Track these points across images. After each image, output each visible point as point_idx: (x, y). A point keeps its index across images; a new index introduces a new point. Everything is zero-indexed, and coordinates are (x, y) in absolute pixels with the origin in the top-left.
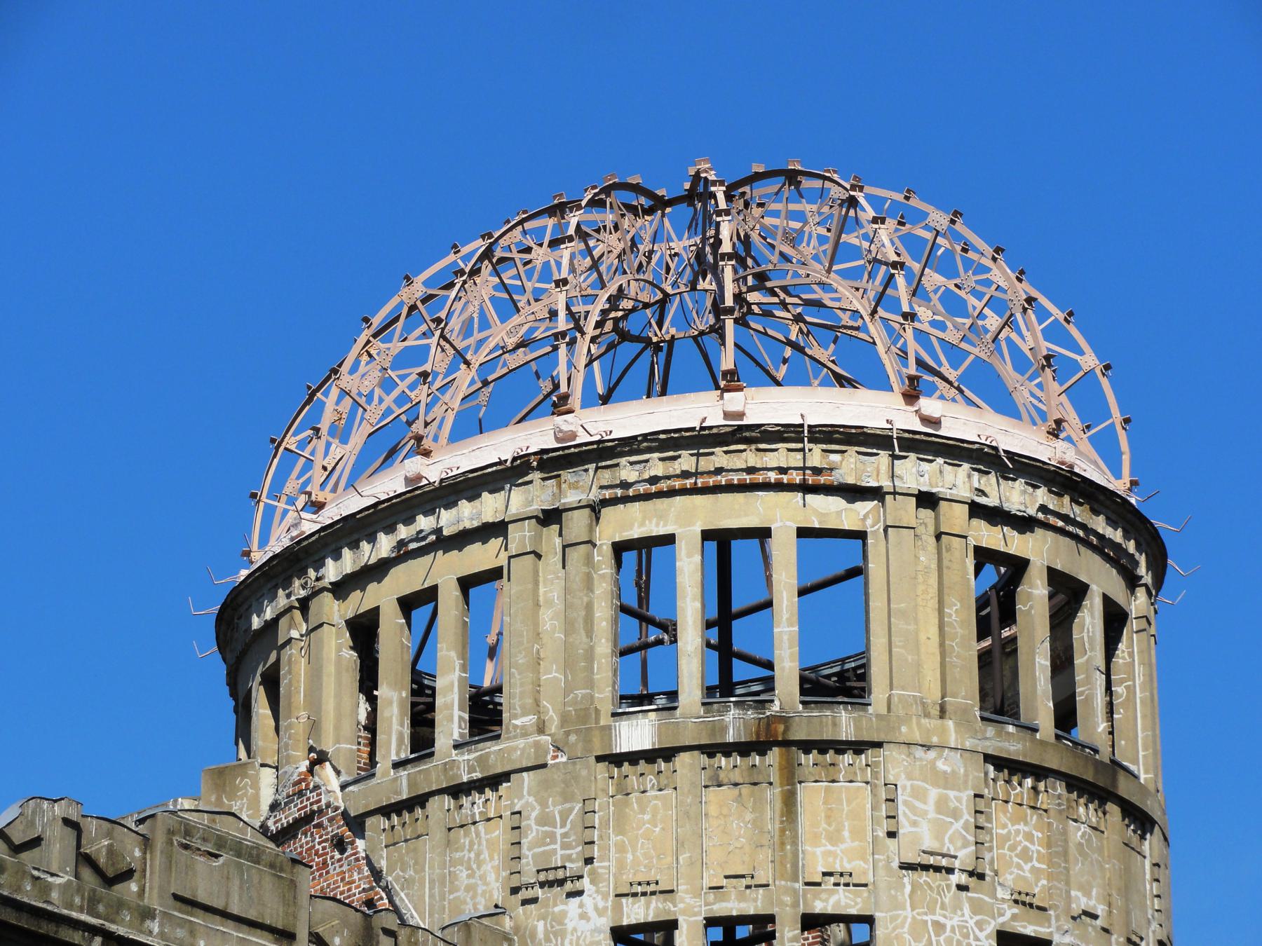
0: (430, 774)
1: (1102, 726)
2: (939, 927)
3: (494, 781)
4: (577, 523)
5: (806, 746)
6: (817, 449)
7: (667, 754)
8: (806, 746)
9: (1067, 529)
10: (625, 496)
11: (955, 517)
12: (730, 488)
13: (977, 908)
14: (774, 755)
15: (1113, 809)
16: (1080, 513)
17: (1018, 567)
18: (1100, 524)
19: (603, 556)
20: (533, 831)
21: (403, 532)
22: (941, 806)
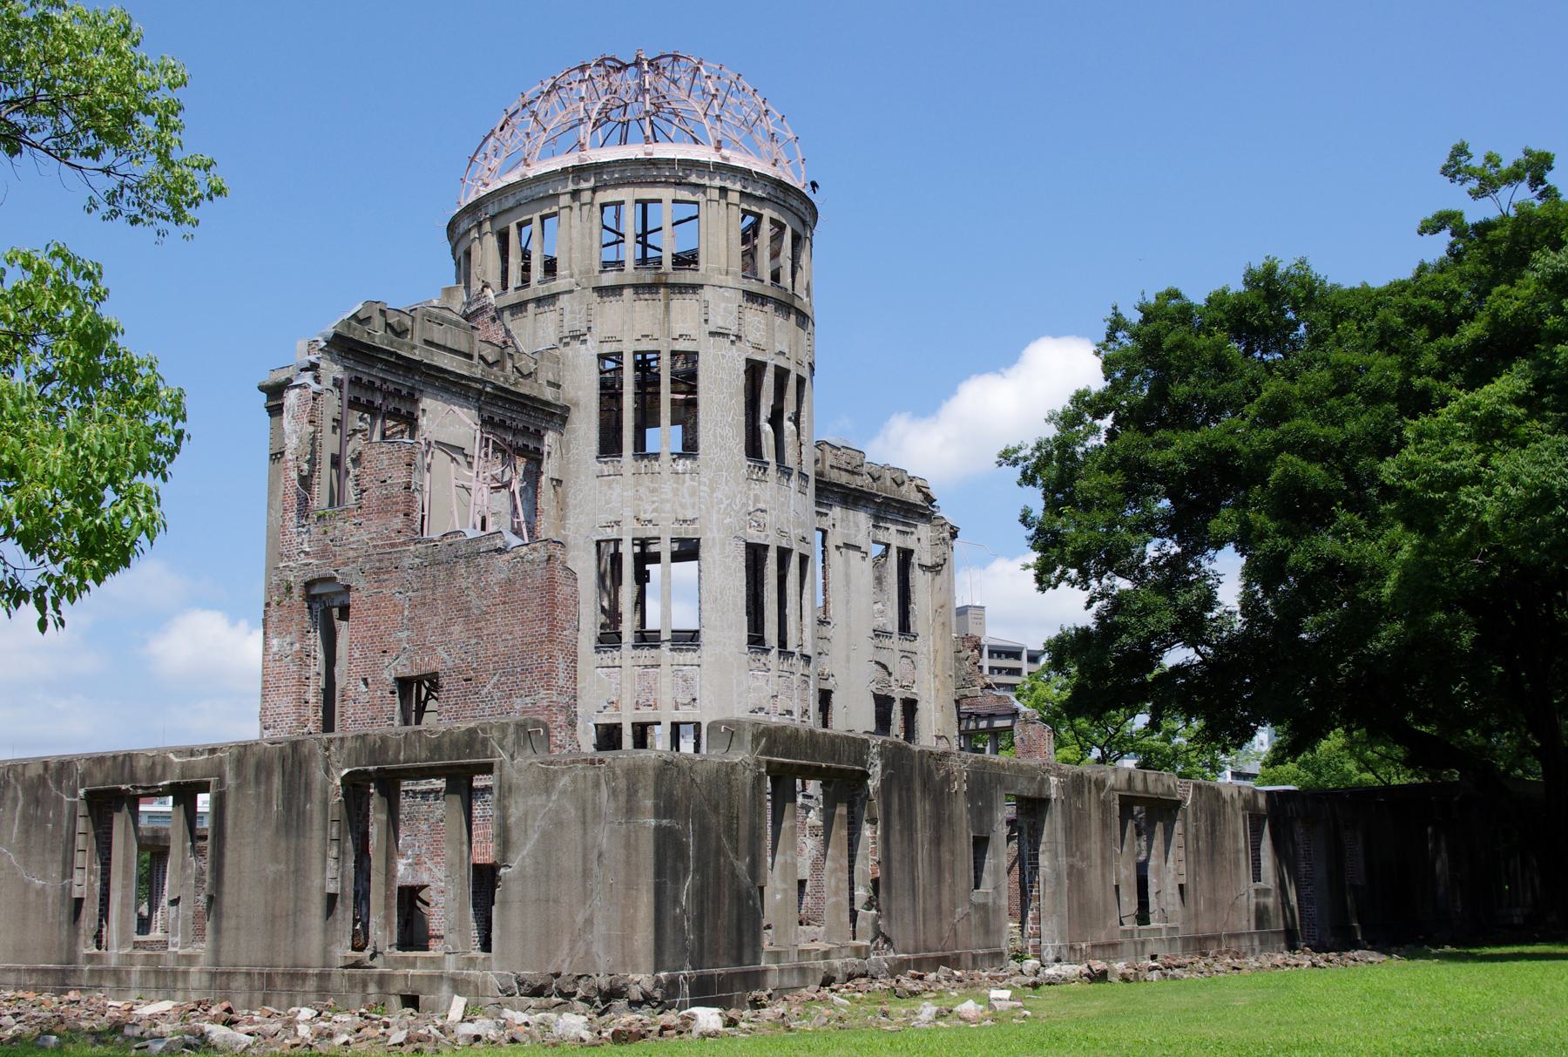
0: (528, 294)
1: (790, 280)
2: (723, 356)
3: (554, 297)
4: (586, 196)
10: (606, 186)
11: (734, 197)
14: (662, 290)
15: (793, 310)
19: (597, 209)
20: (567, 318)
22: (725, 309)
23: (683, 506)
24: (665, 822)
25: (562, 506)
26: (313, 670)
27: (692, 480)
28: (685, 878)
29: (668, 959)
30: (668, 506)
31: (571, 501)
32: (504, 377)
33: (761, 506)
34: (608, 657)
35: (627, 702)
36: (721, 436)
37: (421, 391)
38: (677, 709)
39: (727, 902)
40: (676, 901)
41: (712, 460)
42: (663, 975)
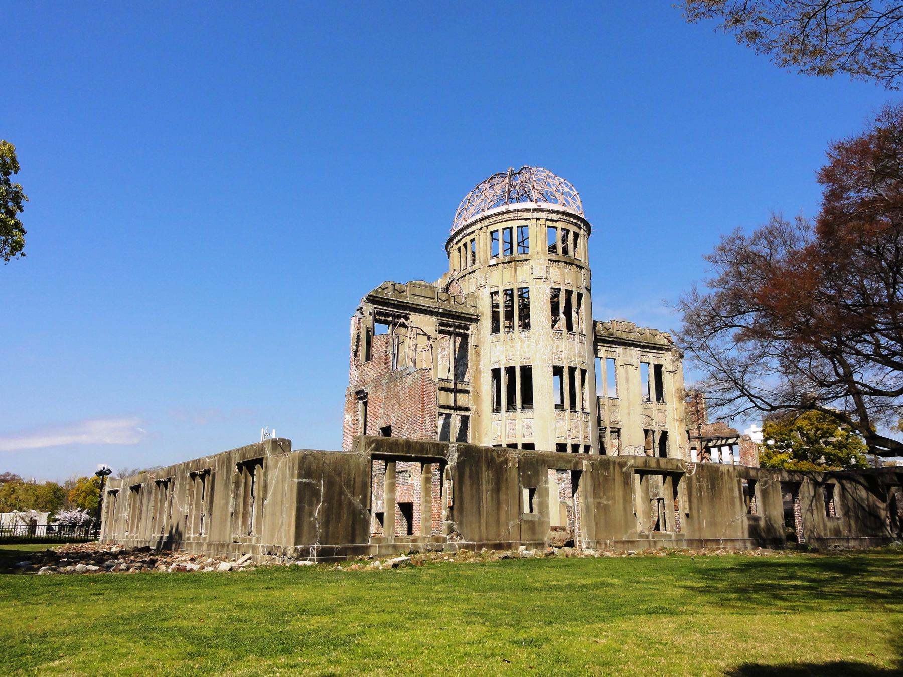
0: (466, 272)
1: (573, 253)
2: (540, 288)
3: (474, 271)
4: (484, 229)
5: (518, 261)
6: (519, 213)
7: (497, 264)
8: (518, 261)
9: (565, 221)
12: (506, 221)
13: (547, 284)
16: (568, 218)
17: (511, 228)
18: (572, 219)
19: (489, 234)
20: (479, 279)
21: (463, 234)
22: (540, 269)
23: (525, 352)
24: (304, 480)
25: (478, 354)
26: (360, 426)
27: (528, 341)
28: (317, 504)
29: (304, 539)
30: (518, 353)
31: (482, 353)
32: (452, 307)
33: (561, 349)
34: (497, 416)
35: (503, 435)
36: (540, 322)
37: (410, 315)
38: (524, 437)
39: (345, 515)
40: (311, 514)
41: (536, 331)
42: (299, 547)
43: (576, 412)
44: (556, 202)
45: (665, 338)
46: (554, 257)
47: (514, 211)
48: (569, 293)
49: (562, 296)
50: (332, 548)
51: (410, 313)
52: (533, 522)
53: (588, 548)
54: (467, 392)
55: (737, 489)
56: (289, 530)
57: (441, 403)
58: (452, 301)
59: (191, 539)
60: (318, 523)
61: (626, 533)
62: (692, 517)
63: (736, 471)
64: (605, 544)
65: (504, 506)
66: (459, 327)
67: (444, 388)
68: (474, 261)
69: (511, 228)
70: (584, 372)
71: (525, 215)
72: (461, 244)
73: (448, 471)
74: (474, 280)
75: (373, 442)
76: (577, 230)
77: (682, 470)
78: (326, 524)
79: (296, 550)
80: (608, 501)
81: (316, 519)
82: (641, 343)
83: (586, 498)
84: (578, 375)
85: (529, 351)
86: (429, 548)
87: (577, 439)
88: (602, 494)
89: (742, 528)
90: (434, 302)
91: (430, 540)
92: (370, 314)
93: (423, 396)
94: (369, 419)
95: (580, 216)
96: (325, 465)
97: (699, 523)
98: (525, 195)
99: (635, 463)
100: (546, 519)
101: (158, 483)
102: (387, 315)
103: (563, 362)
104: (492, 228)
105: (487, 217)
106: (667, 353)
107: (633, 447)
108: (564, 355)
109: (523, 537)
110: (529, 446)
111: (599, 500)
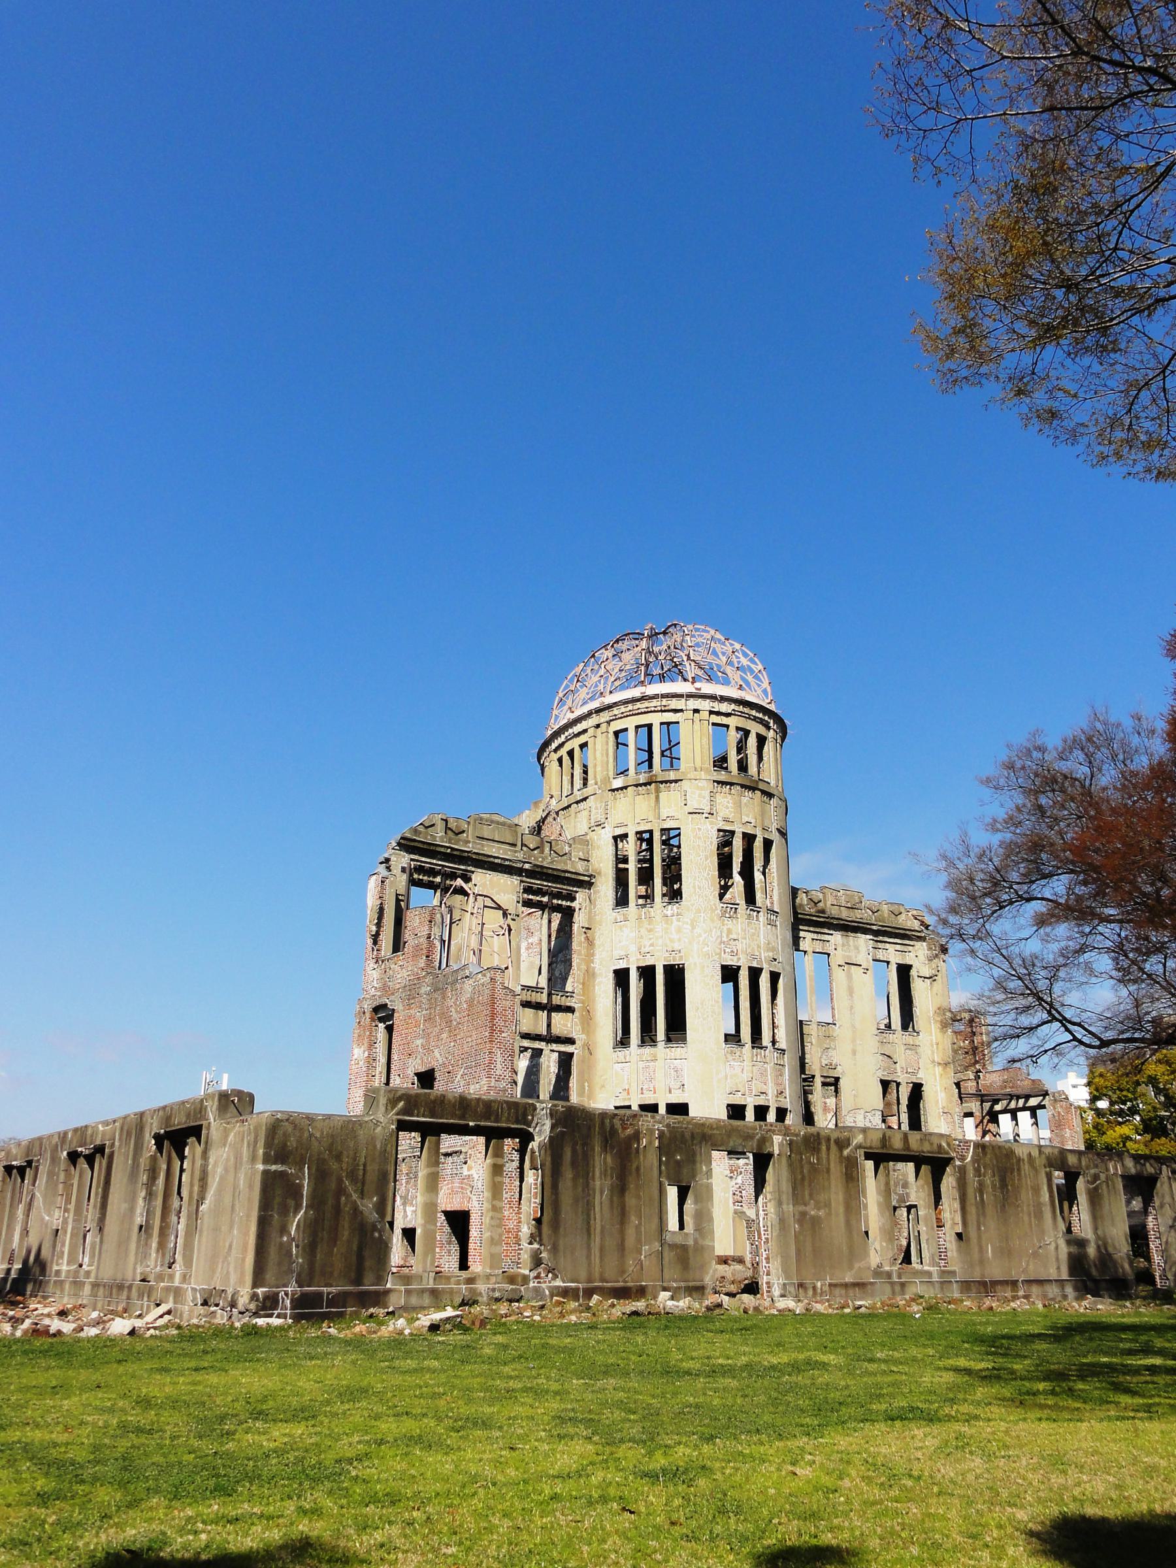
0: (572, 799)
1: (756, 769)
2: (700, 829)
3: (585, 799)
4: (604, 726)
5: (662, 782)
6: (664, 700)
7: (626, 788)
8: (662, 782)
9: (742, 715)
12: (642, 713)
13: (711, 823)
16: (746, 710)
17: (649, 727)
18: (754, 713)
20: (593, 809)
21: (566, 734)
22: (700, 796)
23: (672, 941)
24: (274, 1168)
25: (590, 942)
26: (379, 1069)
27: (678, 920)
29: (269, 1276)
30: (660, 942)
31: (597, 942)
32: (546, 860)
34: (622, 1053)
35: (634, 1089)
36: (700, 888)
37: (473, 872)
38: (670, 1092)
39: (346, 1233)
40: (284, 1230)
41: (693, 905)
42: (260, 1291)
43: (761, 1048)
44: (726, 682)
45: (916, 919)
46: (723, 776)
47: (655, 697)
48: (749, 839)
49: (738, 844)
50: (320, 1294)
51: (473, 869)
52: (684, 1248)
53: (782, 1296)
54: (570, 1010)
55: (1045, 1188)
56: (243, 1260)
57: (525, 1029)
58: (547, 850)
59: (63, 1274)
60: (297, 1246)
61: (851, 1267)
62: (968, 1240)
63: (1044, 1156)
64: (814, 1288)
65: (633, 1218)
66: (559, 896)
67: (530, 1002)
68: (585, 784)
69: (649, 727)
70: (775, 977)
71: (674, 704)
72: (563, 752)
73: (533, 1152)
74: (585, 813)
75: (400, 1099)
76: (762, 730)
77: (948, 1153)
78: (311, 1248)
79: (254, 1297)
80: (819, 1209)
81: (293, 1239)
82: (874, 928)
83: (780, 1203)
84: (764, 982)
85: (679, 940)
86: (497, 1295)
87: (763, 1097)
88: (807, 1197)
89: (1057, 1259)
90: (516, 852)
91: (500, 1279)
92: (403, 870)
93: (493, 1016)
94: (395, 1057)
95: (767, 706)
96: (313, 1139)
97: (982, 1250)
98: (674, 669)
99: (865, 1138)
100: (707, 1242)
101: (8, 1169)
102: (432, 872)
103: (739, 959)
104: (617, 725)
105: (609, 707)
106: (918, 944)
107: (862, 1112)
108: (740, 946)
109: (666, 1276)
110: (678, 1109)
111: (802, 1208)
